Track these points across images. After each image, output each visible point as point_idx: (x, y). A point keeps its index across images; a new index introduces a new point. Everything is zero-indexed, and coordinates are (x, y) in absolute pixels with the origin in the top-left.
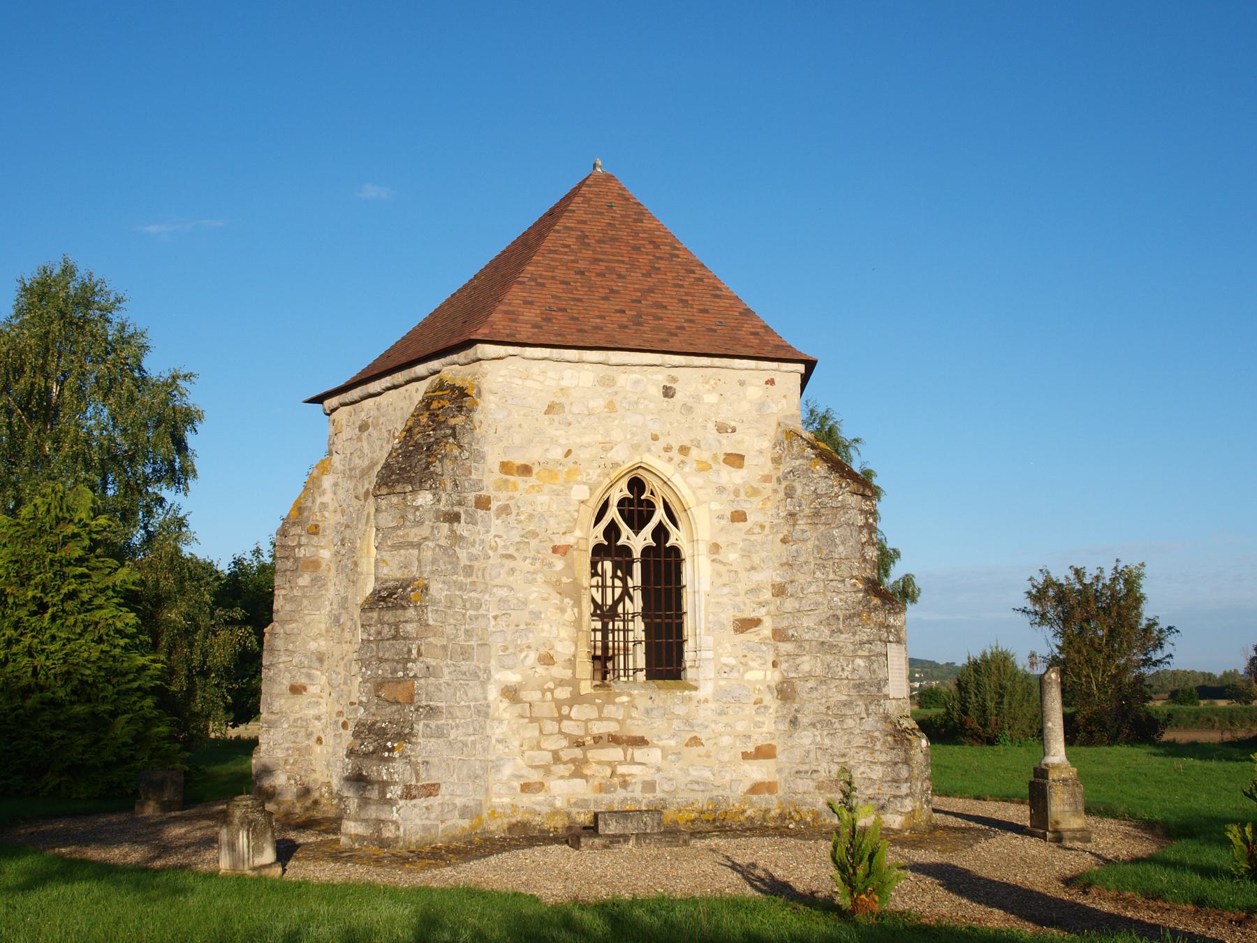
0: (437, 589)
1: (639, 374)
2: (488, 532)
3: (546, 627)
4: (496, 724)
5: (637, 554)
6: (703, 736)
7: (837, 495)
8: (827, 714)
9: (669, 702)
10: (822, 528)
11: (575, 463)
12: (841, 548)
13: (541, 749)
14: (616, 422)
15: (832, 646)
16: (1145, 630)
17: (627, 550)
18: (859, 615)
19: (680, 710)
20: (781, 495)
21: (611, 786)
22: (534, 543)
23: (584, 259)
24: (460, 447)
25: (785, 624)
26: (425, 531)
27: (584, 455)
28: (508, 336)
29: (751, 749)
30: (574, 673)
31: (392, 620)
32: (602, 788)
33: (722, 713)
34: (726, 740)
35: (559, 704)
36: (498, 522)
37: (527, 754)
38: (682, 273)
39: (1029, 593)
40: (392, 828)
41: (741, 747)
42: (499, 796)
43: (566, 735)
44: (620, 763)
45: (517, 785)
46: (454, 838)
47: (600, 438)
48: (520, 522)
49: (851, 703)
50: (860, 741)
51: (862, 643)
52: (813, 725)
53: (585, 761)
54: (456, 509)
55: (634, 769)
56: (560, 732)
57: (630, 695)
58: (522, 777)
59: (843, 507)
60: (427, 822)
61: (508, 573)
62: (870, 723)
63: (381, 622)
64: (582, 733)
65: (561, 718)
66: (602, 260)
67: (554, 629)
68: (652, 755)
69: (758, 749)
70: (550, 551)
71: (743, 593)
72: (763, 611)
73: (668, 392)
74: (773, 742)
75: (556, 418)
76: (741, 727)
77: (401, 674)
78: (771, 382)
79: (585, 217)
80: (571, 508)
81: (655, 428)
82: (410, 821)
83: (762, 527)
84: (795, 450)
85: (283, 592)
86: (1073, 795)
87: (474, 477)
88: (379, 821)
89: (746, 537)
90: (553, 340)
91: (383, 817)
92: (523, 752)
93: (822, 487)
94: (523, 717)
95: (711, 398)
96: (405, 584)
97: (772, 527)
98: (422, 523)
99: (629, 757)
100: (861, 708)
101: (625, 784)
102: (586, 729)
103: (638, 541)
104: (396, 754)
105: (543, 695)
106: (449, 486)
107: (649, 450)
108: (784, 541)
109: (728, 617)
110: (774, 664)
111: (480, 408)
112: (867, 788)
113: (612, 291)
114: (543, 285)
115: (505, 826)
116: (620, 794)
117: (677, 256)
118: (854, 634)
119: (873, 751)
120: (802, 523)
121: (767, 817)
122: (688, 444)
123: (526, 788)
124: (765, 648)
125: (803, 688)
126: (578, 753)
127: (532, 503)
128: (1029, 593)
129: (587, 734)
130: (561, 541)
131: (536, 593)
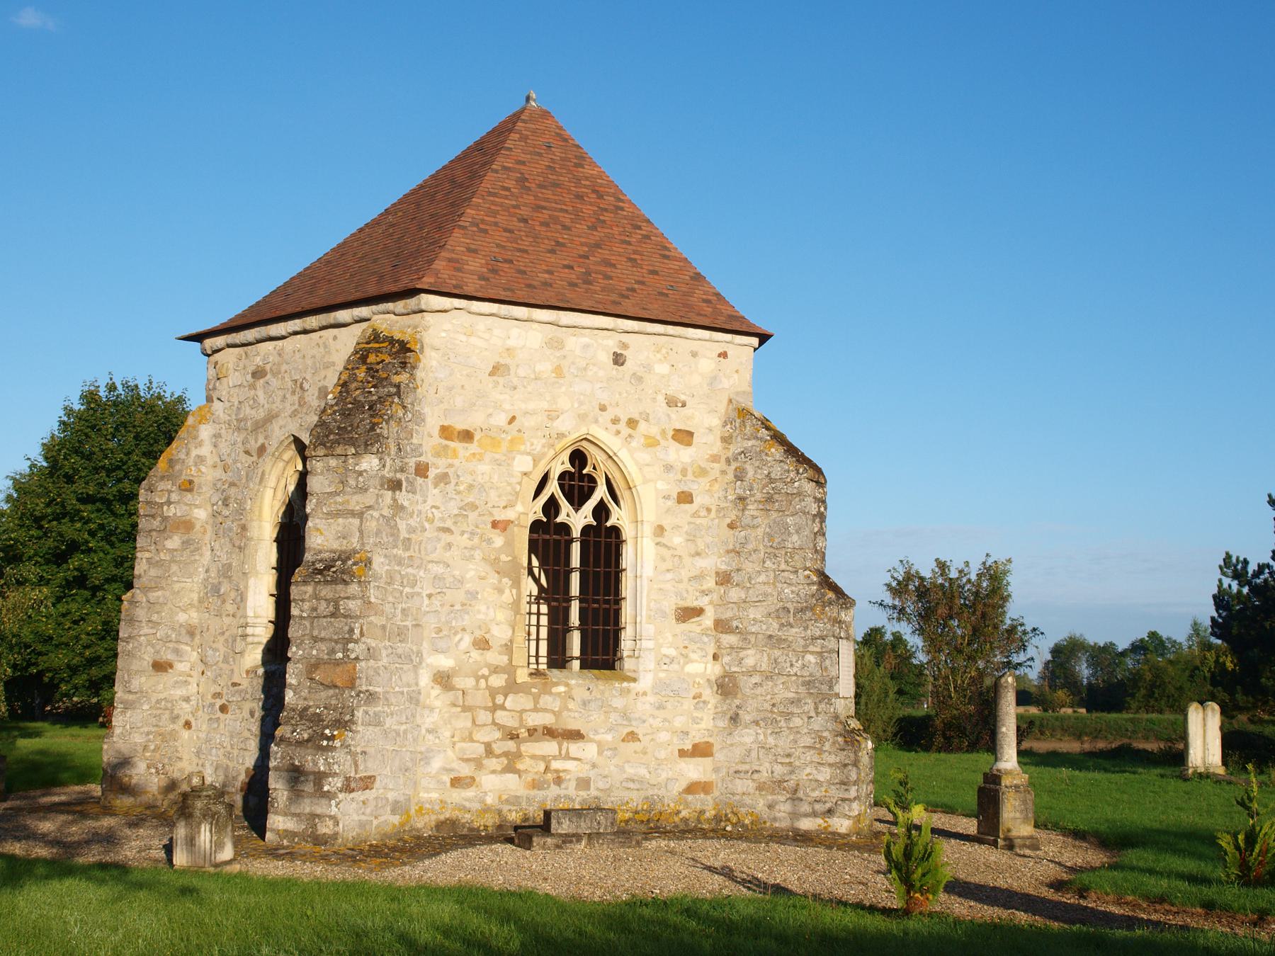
0: (380, 564)
1: (589, 338)
2: (425, 502)
3: (483, 608)
4: (426, 712)
5: (576, 533)
6: (640, 732)
7: (792, 481)
8: (772, 712)
9: (607, 694)
10: (774, 515)
11: (519, 431)
12: (795, 538)
13: (472, 740)
14: (563, 389)
15: (780, 640)
16: (1007, 631)
17: (565, 528)
18: (812, 609)
19: (618, 702)
20: (730, 477)
21: (545, 782)
22: (472, 516)
23: (525, 205)
24: (404, 407)
25: (729, 614)
26: (369, 499)
27: (527, 422)
28: (455, 287)
29: (688, 747)
30: (511, 660)
31: (330, 595)
32: (535, 785)
33: (661, 707)
34: (664, 736)
35: (493, 692)
36: (436, 491)
37: (459, 745)
38: (629, 228)
39: (888, 585)
40: (330, 823)
41: (678, 744)
42: (427, 790)
43: (500, 727)
44: (555, 758)
45: (446, 779)
46: (386, 835)
47: (545, 405)
48: (459, 493)
49: (799, 700)
50: (808, 741)
51: (814, 638)
52: (756, 723)
53: (519, 755)
54: (399, 476)
55: (569, 765)
56: (494, 723)
57: (567, 685)
58: (452, 770)
59: (799, 494)
60: (363, 818)
61: (444, 548)
62: (818, 723)
63: (316, 596)
64: (516, 725)
65: (495, 708)
66: (544, 208)
67: (491, 610)
68: (586, 750)
69: (695, 746)
70: (489, 526)
71: (686, 580)
72: (706, 599)
73: (618, 360)
74: (710, 740)
75: (501, 380)
76: (679, 722)
77: (340, 655)
78: (724, 355)
79: (523, 157)
80: (514, 481)
81: (604, 397)
82: (351, 816)
83: (709, 510)
84: (748, 430)
85: (147, 555)
86: (1024, 802)
87: (415, 441)
88: (314, 816)
89: (692, 520)
90: (503, 295)
91: (319, 811)
92: (454, 744)
93: (777, 471)
94: (455, 705)
95: (662, 369)
96: (344, 557)
97: (718, 511)
98: (366, 490)
99: (563, 752)
100: (809, 706)
101: (558, 781)
102: (521, 720)
103: (578, 519)
104: (337, 743)
105: (477, 682)
106: (393, 450)
107: (596, 421)
108: (731, 526)
109: (670, 604)
110: (715, 657)
111: (421, 365)
112: (813, 790)
113: (558, 244)
114: (486, 231)
115: (433, 824)
116: (554, 791)
117: (622, 209)
118: (806, 628)
119: (821, 752)
120: (752, 508)
121: (702, 818)
122: (636, 416)
123: (456, 782)
124: (705, 639)
125: (746, 683)
126: (511, 745)
127: (473, 473)
128: (888, 585)
129: (522, 726)
130: (500, 516)
131: (473, 571)
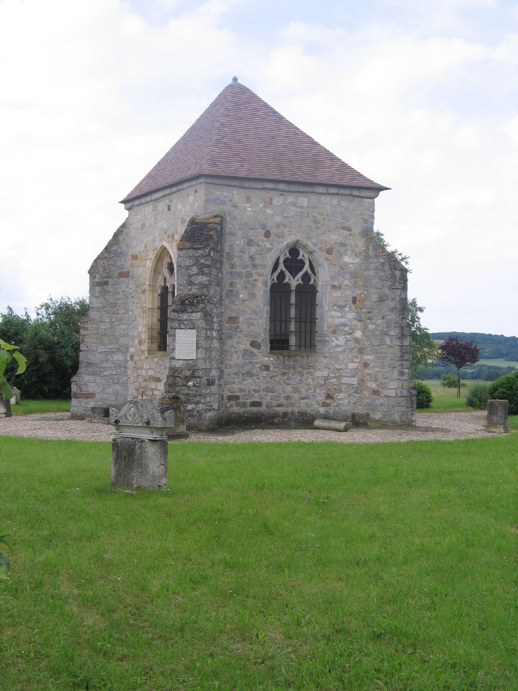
54: (105, 280)
78: (196, 192)
87: (119, 264)
111: (124, 233)
